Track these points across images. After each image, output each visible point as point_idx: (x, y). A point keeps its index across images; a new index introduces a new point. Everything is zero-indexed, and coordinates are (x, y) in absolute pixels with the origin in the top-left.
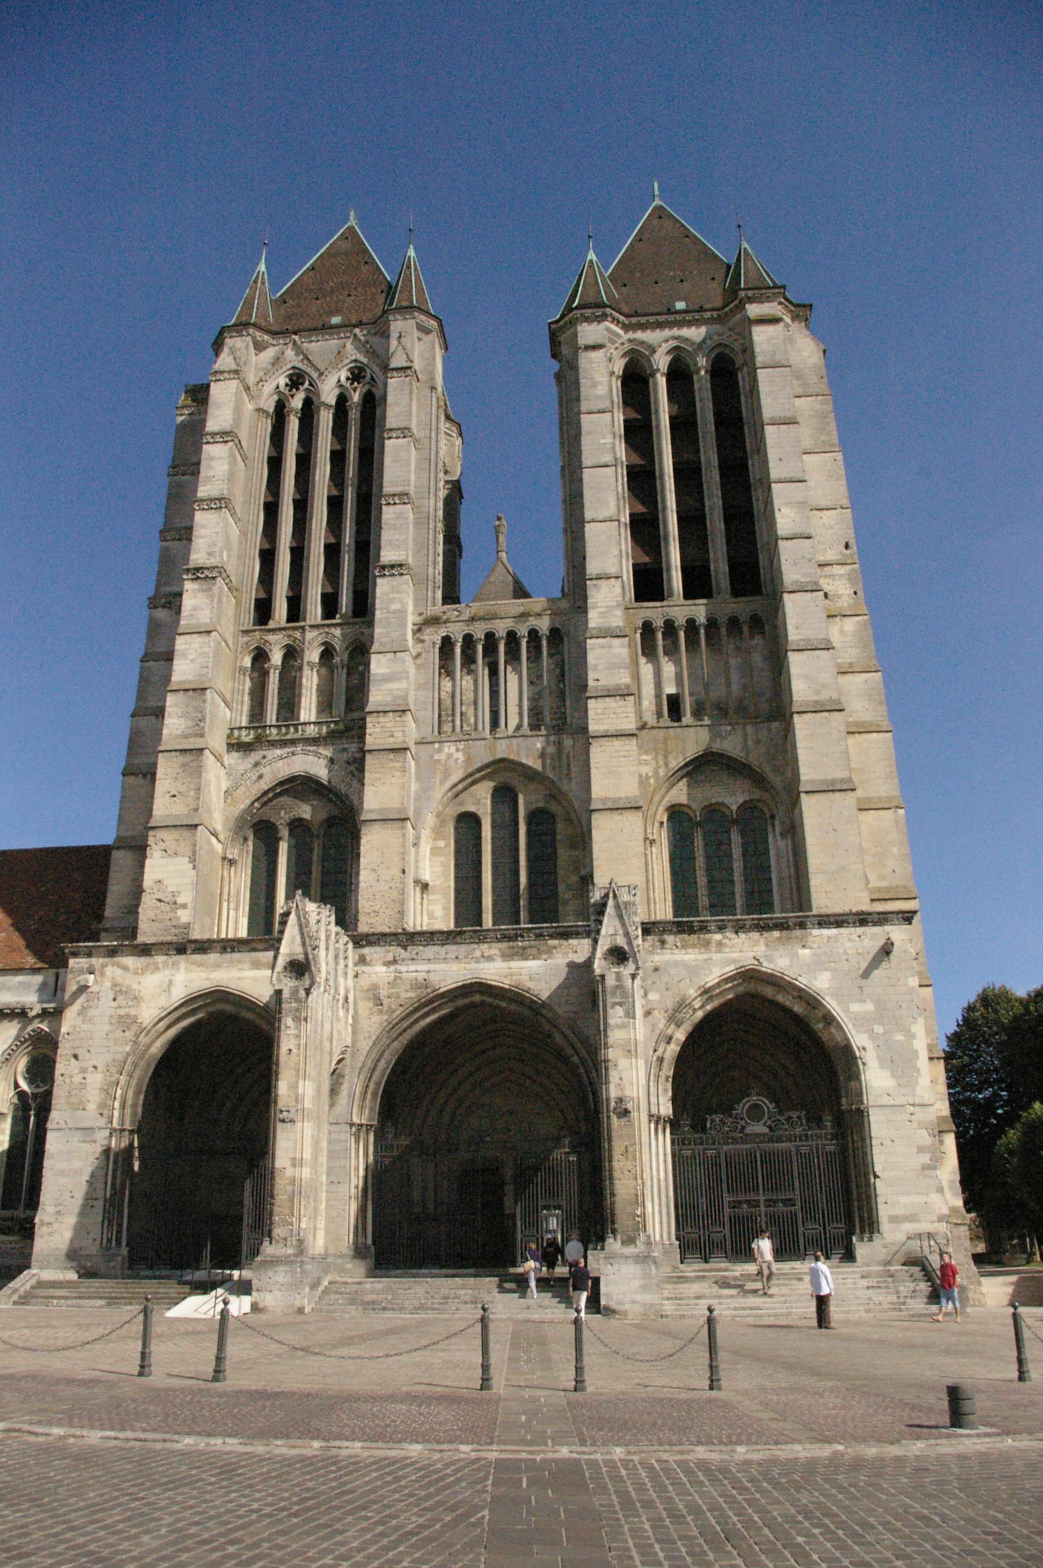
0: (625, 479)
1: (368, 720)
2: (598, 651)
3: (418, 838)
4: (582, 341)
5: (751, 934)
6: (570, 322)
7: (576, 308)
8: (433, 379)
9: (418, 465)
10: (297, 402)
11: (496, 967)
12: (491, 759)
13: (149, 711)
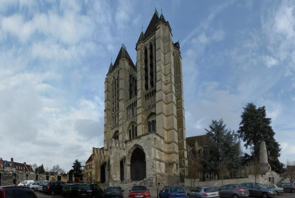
10: (114, 81)
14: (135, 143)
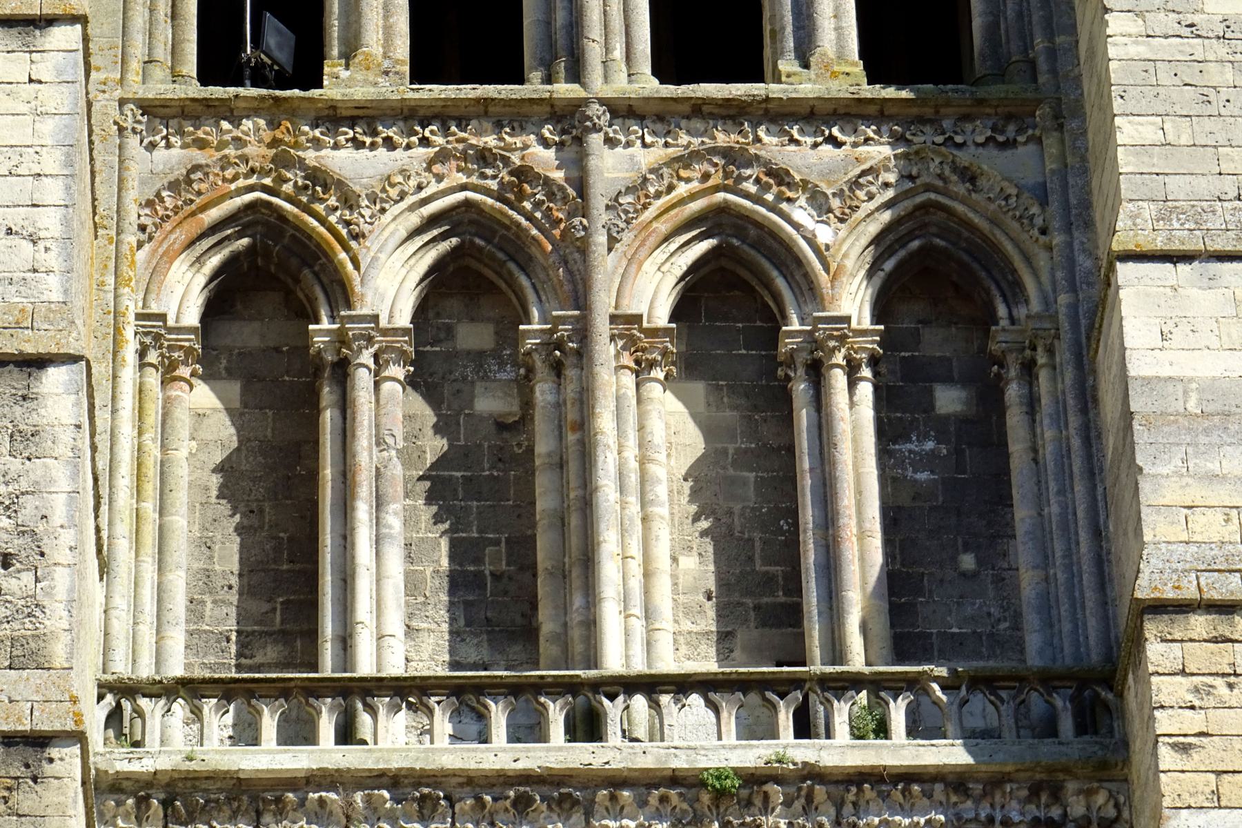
1: (1157, 653)
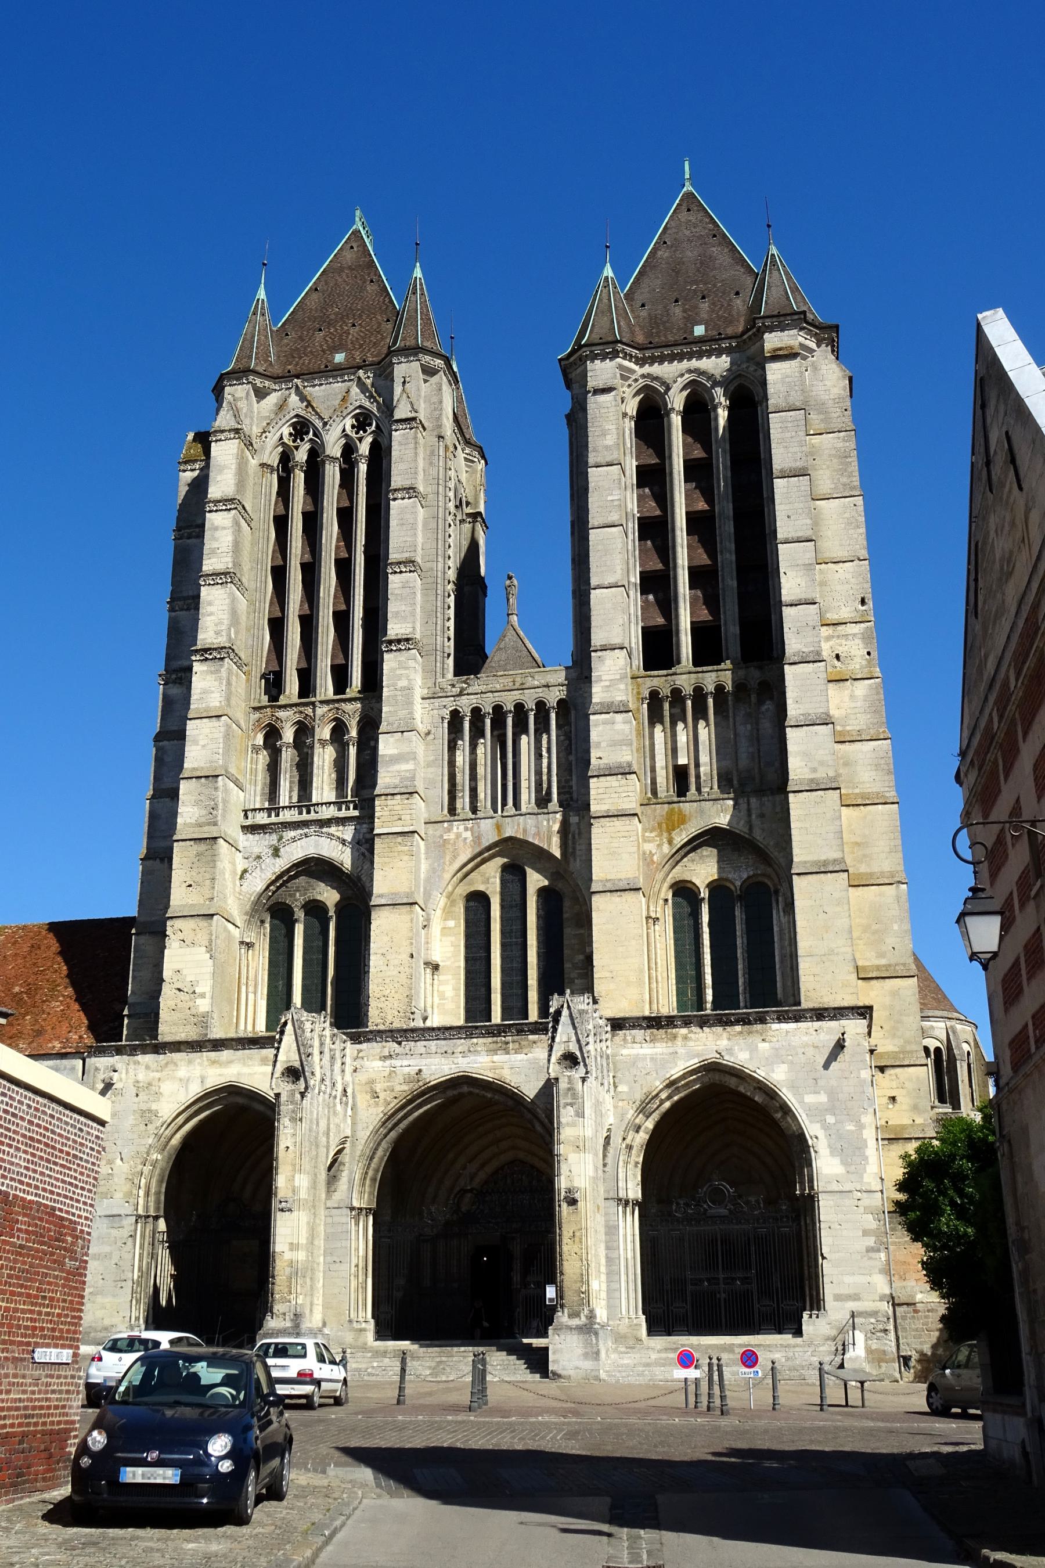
0: (637, 534)
2: (601, 728)
3: (428, 919)
4: (591, 383)
5: (714, 1029)
6: (580, 360)
7: (585, 345)
8: (440, 426)
9: (425, 524)
10: (301, 455)
11: (483, 1061)
12: (497, 839)
13: (166, 795)
14: (711, 1056)
